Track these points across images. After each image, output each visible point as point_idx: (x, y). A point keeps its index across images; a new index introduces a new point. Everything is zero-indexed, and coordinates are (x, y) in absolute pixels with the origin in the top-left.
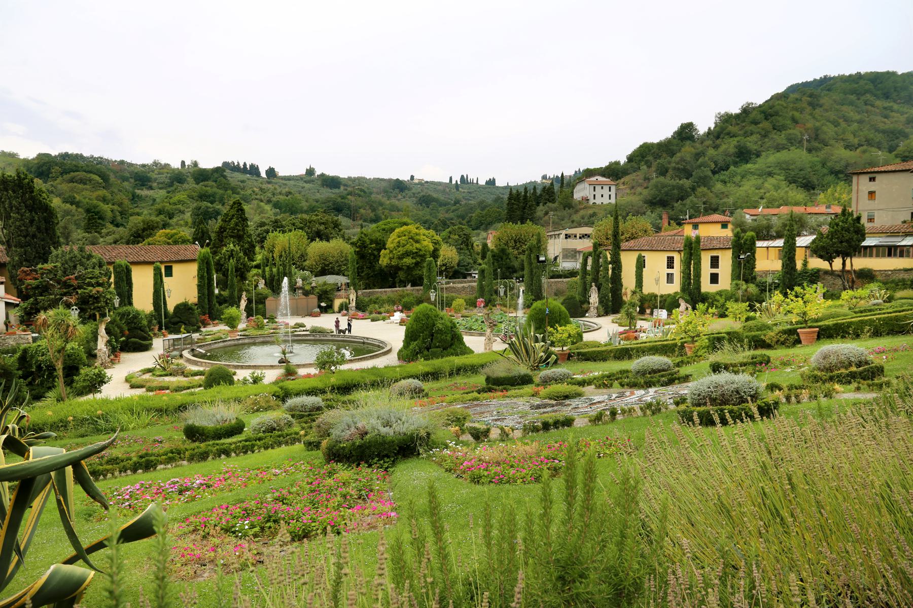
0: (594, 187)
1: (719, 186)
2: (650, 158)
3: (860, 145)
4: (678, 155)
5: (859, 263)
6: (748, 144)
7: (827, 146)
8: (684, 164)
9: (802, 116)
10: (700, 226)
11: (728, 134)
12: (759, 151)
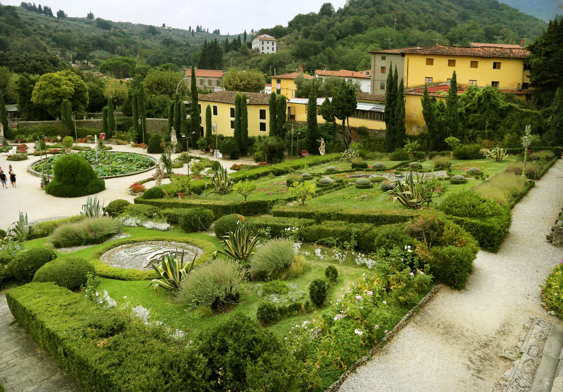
0: (263, 42)
1: (340, 47)
2: (300, 25)
3: (428, 28)
4: (317, 24)
5: (354, 122)
6: (361, 21)
7: (408, 26)
8: (320, 31)
9: (396, 6)
10: (282, 81)
11: (350, 13)
12: (368, 26)
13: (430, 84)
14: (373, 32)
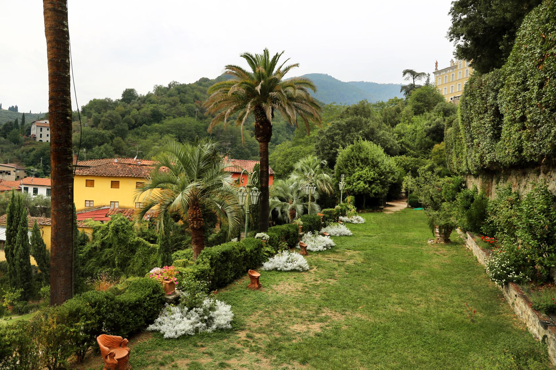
6: (161, 110)
9: (202, 95)
11: (150, 101)
13: (90, 208)
14: (168, 122)
